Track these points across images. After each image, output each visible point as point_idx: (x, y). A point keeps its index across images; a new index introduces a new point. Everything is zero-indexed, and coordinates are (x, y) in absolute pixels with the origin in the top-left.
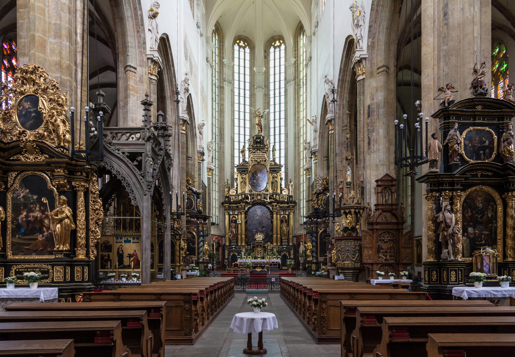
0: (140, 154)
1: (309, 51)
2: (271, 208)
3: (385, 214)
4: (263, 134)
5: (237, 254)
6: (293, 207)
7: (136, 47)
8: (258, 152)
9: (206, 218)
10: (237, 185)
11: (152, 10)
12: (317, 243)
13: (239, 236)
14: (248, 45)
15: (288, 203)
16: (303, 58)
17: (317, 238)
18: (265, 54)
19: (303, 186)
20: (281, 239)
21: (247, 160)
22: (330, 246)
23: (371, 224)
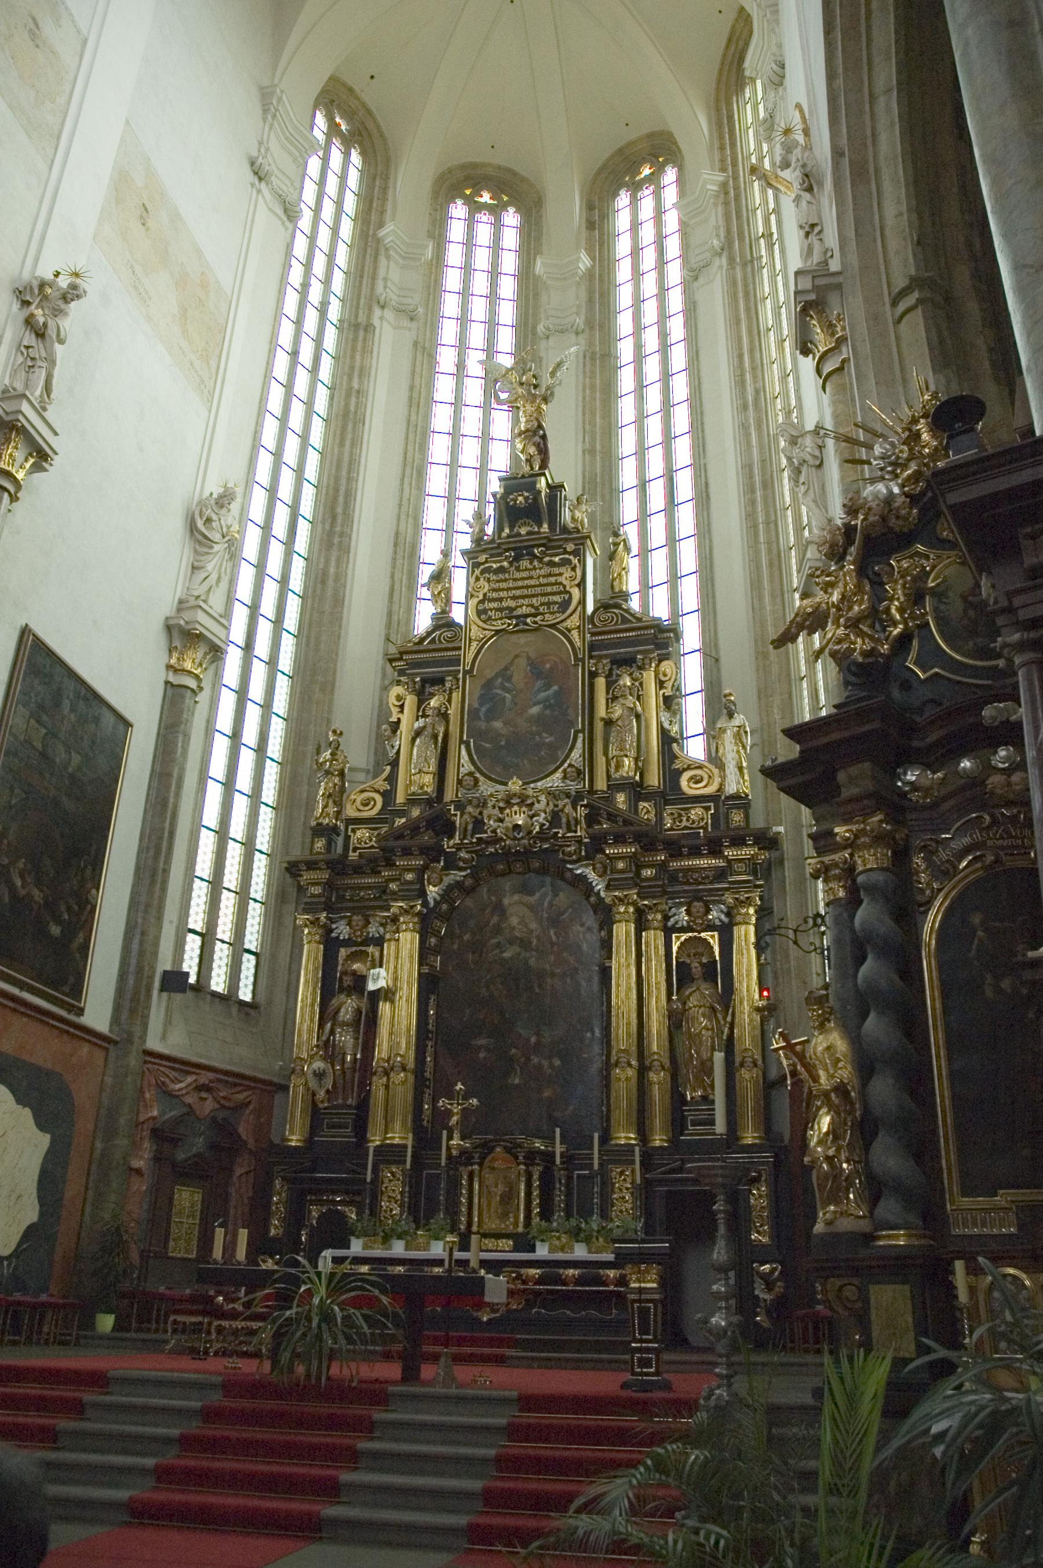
8: (525, 563)
15: (715, 849)
21: (458, 614)
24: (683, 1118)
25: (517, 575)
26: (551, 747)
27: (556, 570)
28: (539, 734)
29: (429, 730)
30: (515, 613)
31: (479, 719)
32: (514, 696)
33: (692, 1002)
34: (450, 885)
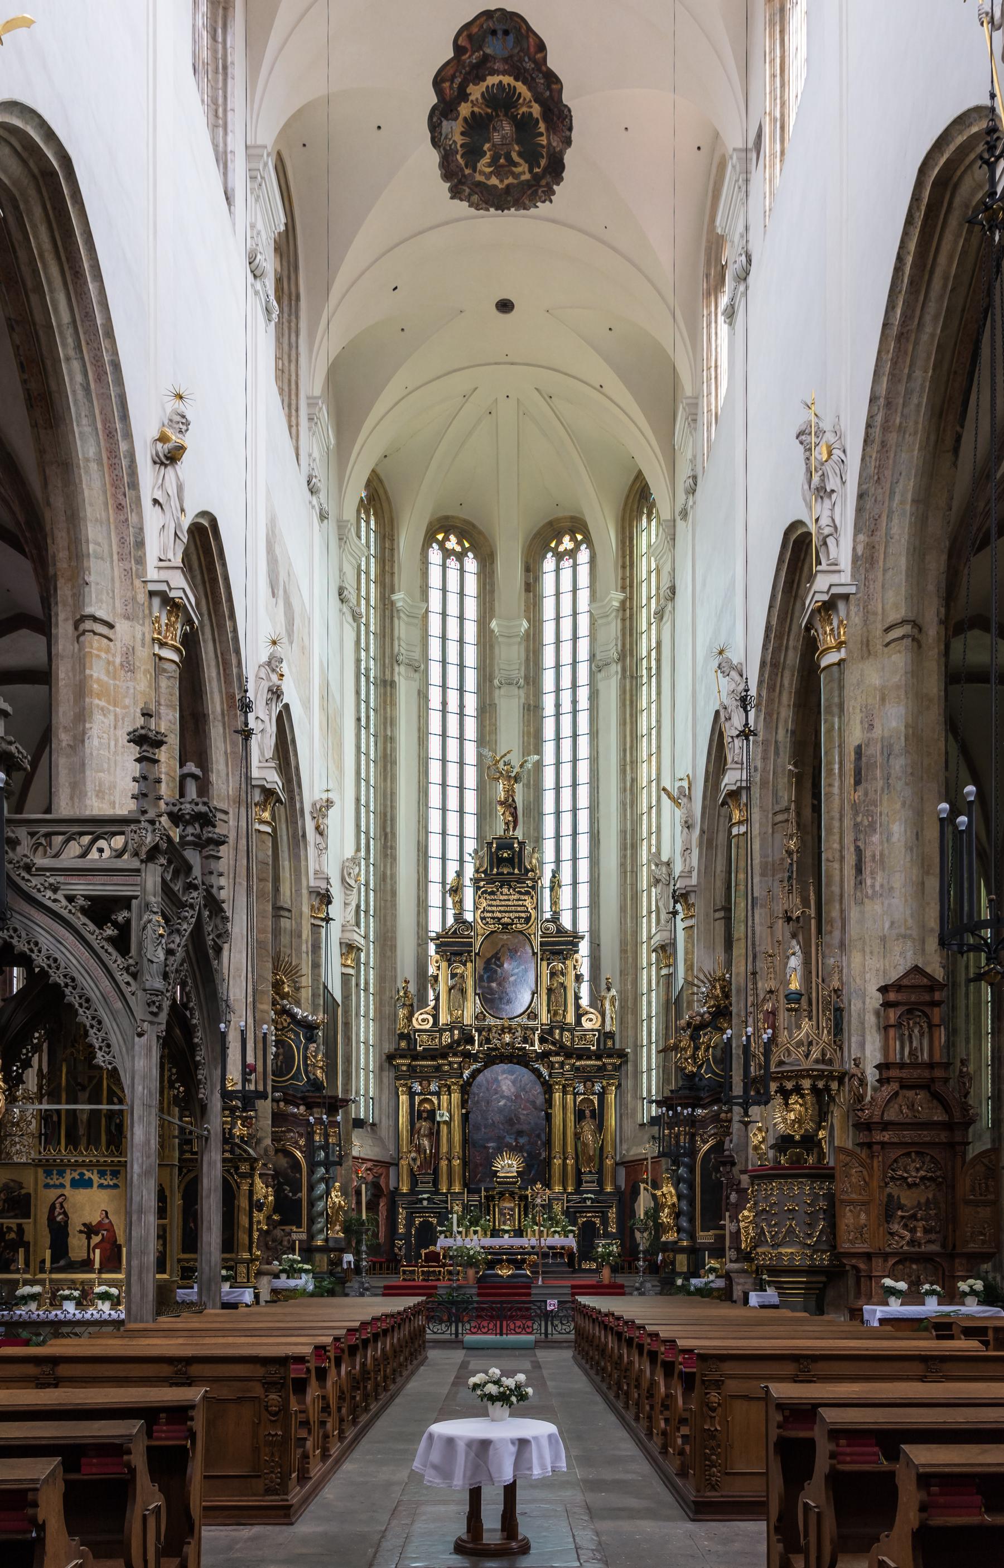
0: (125, 902)
1: (667, 569)
2: (545, 1072)
3: (910, 1094)
4: (519, 833)
5: (435, 1221)
6: (617, 1068)
7: (111, 557)
8: (505, 890)
9: (335, 1105)
10: (437, 999)
11: (163, 438)
12: (691, 1187)
13: (444, 1163)
14: (473, 548)
15: (599, 1058)
16: (647, 591)
17: (692, 1170)
18: (527, 577)
19: (649, 1003)
20: (579, 1173)
21: (469, 917)
22: (733, 1197)
23: (864, 1126)
33: (586, 1128)
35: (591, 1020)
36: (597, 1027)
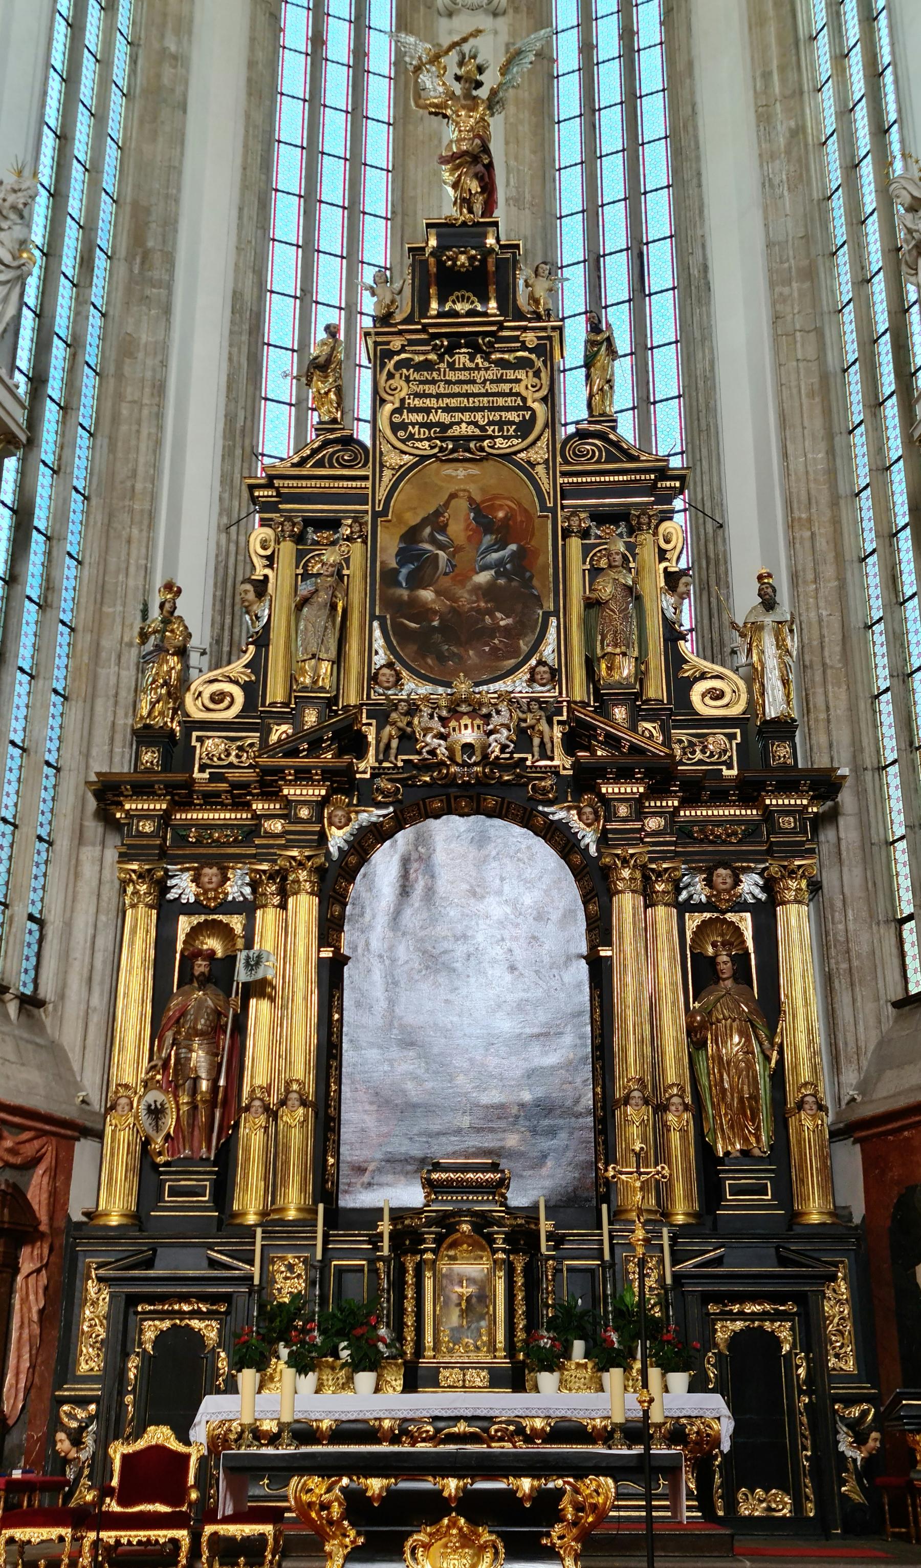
2: (589, 838)
24: (720, 1183)
25: (452, 376)
26: (507, 631)
27: (510, 374)
28: (491, 613)
29: (323, 597)
30: (450, 433)
31: (400, 585)
32: (452, 555)
34: (361, 828)
35: (717, 695)
36: (736, 710)
